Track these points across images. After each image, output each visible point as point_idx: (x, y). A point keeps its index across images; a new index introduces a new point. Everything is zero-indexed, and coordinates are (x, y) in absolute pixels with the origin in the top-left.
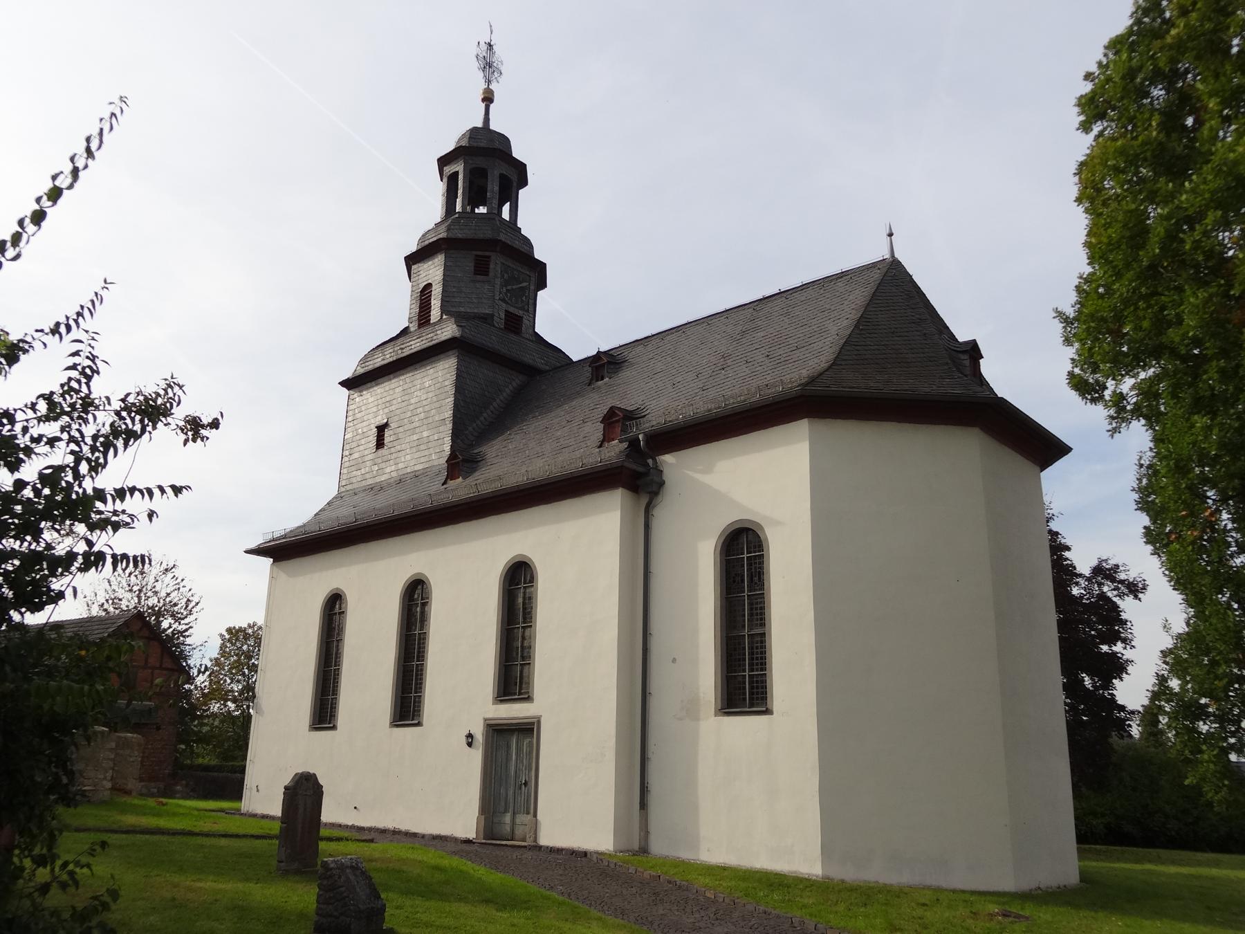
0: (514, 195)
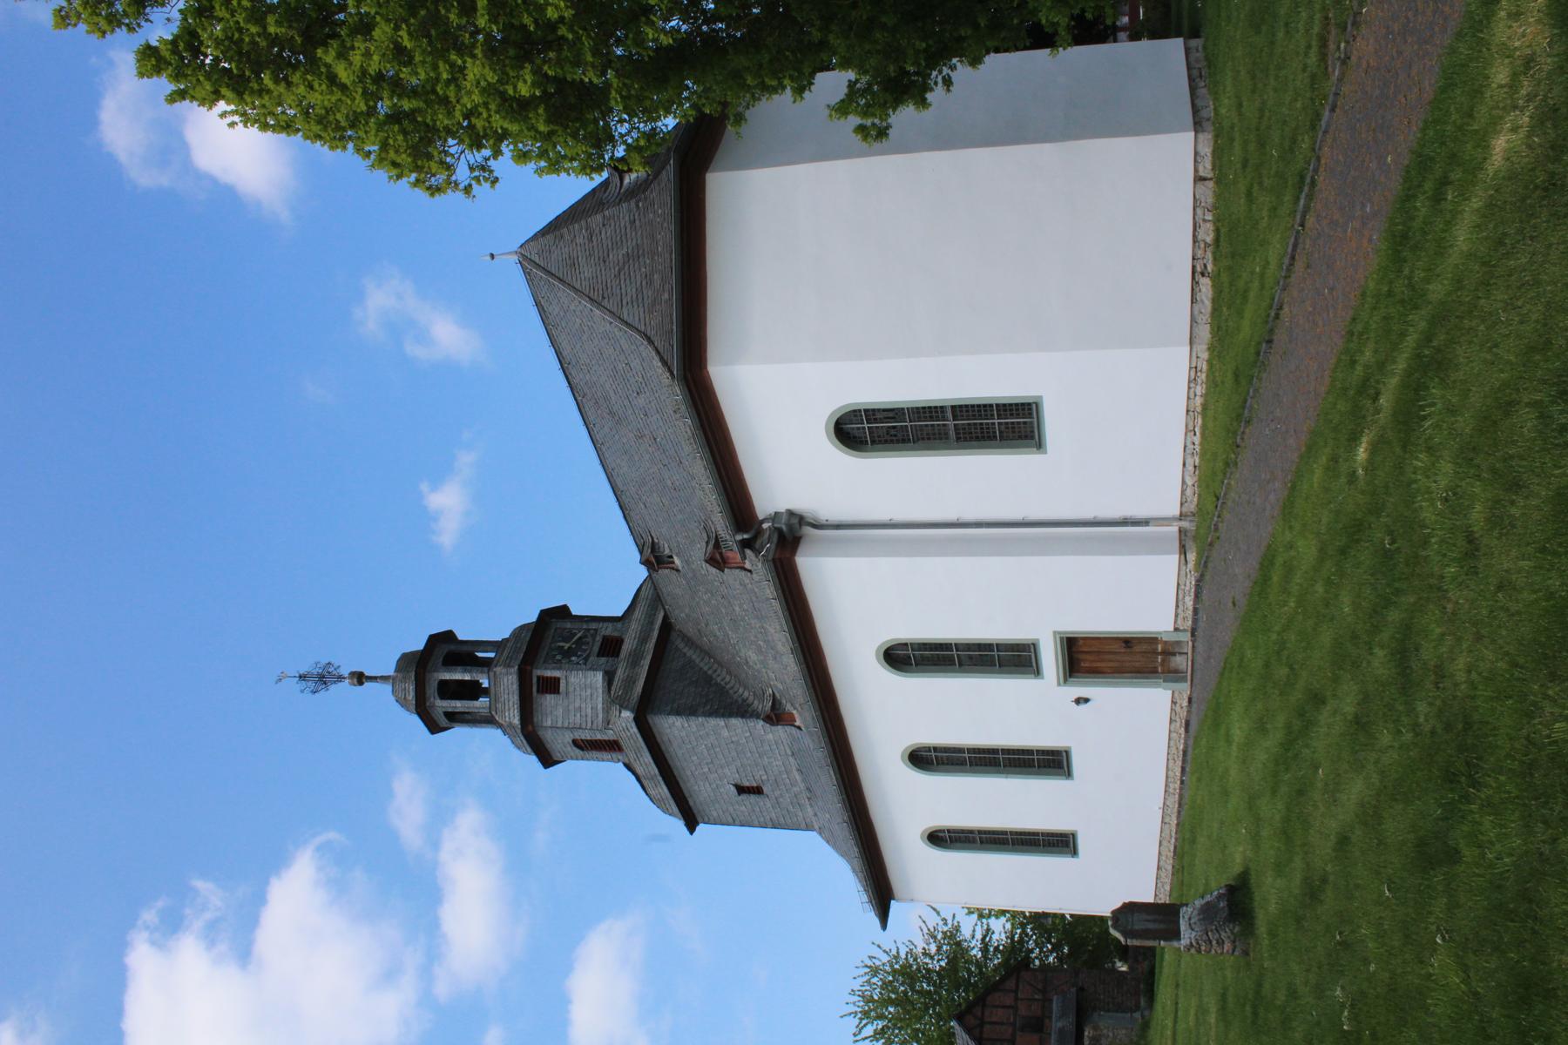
0: (465, 648)
